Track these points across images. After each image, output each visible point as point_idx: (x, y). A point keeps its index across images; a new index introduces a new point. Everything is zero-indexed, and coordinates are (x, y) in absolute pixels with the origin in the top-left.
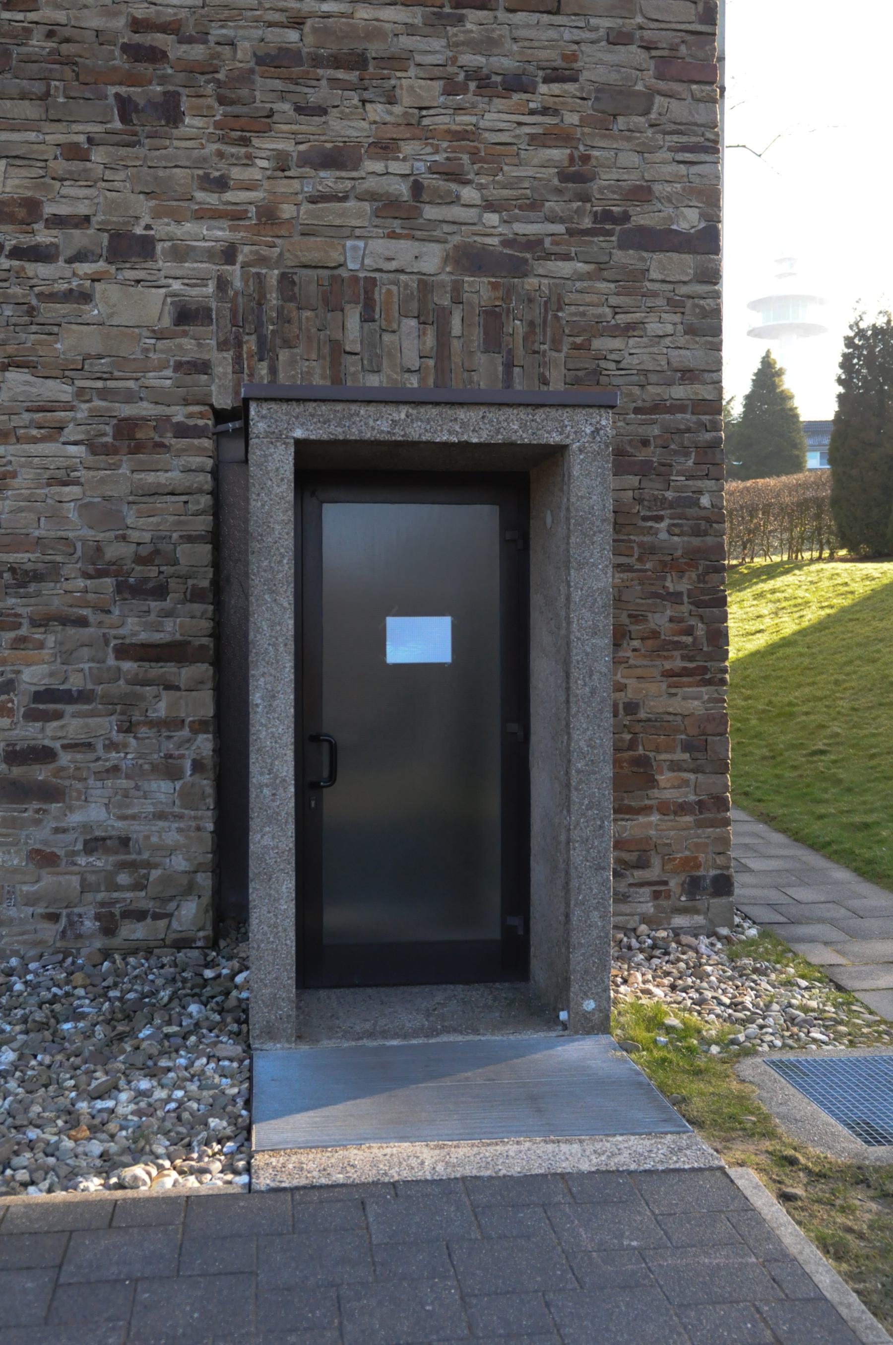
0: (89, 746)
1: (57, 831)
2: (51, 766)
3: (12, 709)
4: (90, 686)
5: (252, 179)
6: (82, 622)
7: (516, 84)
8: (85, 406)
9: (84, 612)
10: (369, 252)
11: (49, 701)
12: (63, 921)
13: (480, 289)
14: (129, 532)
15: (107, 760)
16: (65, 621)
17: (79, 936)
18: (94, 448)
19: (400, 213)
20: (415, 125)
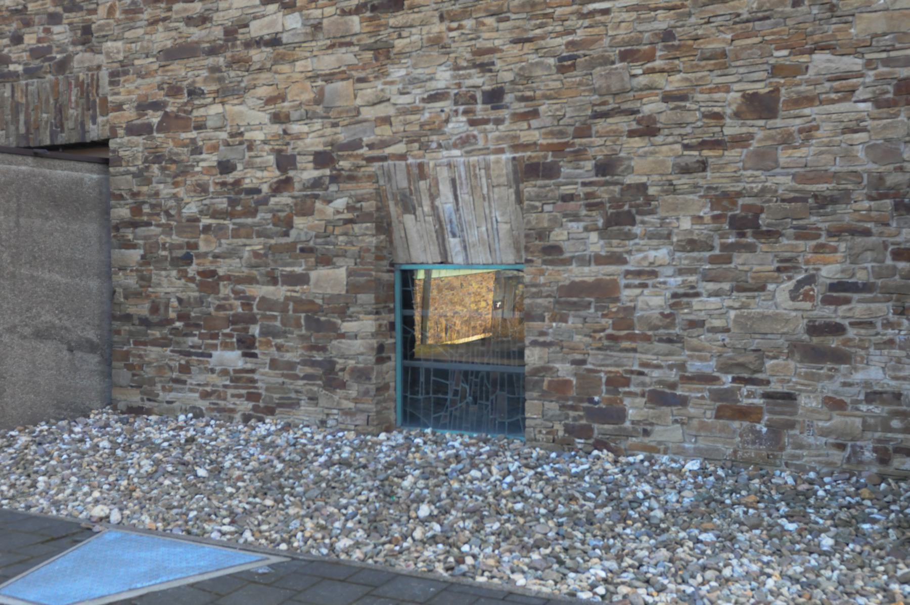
0: (871, 324)
1: (845, 384)
2: (841, 338)
3: (813, 296)
4: (872, 280)
6: (867, 233)
8: (871, 73)
9: (869, 225)
11: (840, 290)
12: (849, 450)
14: (905, 164)
15: (885, 335)
16: (854, 232)
17: (861, 463)
18: (878, 103)
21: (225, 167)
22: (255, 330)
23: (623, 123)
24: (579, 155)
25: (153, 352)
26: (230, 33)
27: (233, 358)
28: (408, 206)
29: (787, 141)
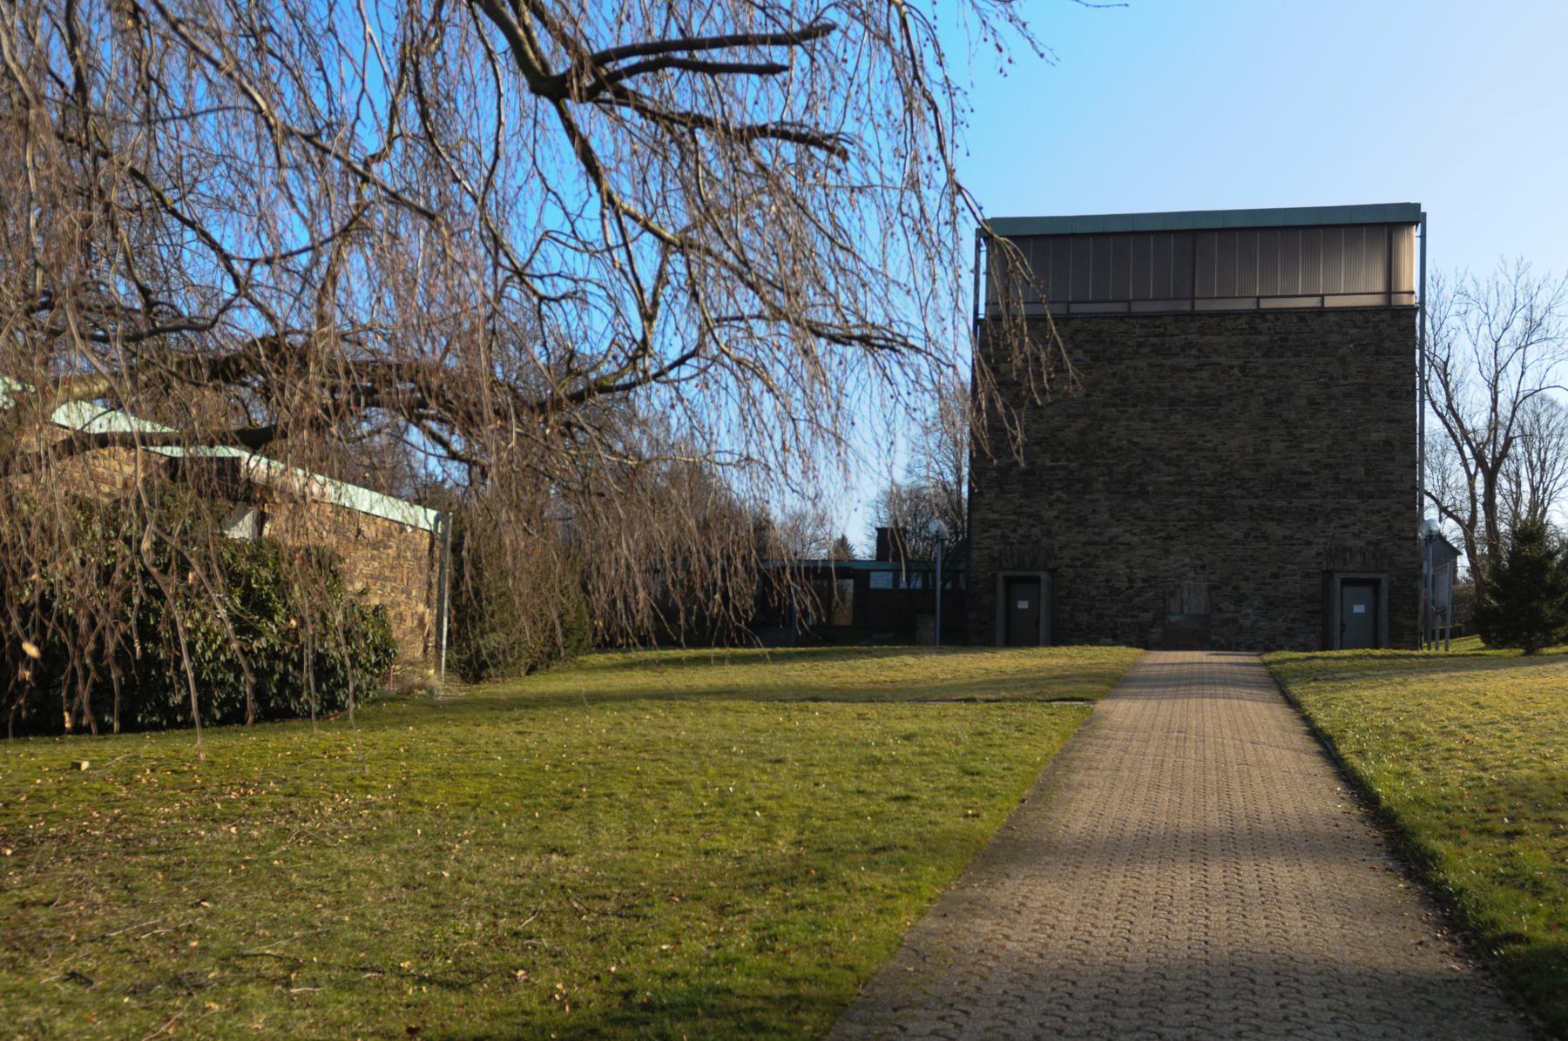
7: (1379, 512)
10: (1351, 542)
11: (1294, 620)
13: (1371, 548)
19: (1356, 535)
21: (1108, 581)
26: (1111, 539)
28: (1172, 595)
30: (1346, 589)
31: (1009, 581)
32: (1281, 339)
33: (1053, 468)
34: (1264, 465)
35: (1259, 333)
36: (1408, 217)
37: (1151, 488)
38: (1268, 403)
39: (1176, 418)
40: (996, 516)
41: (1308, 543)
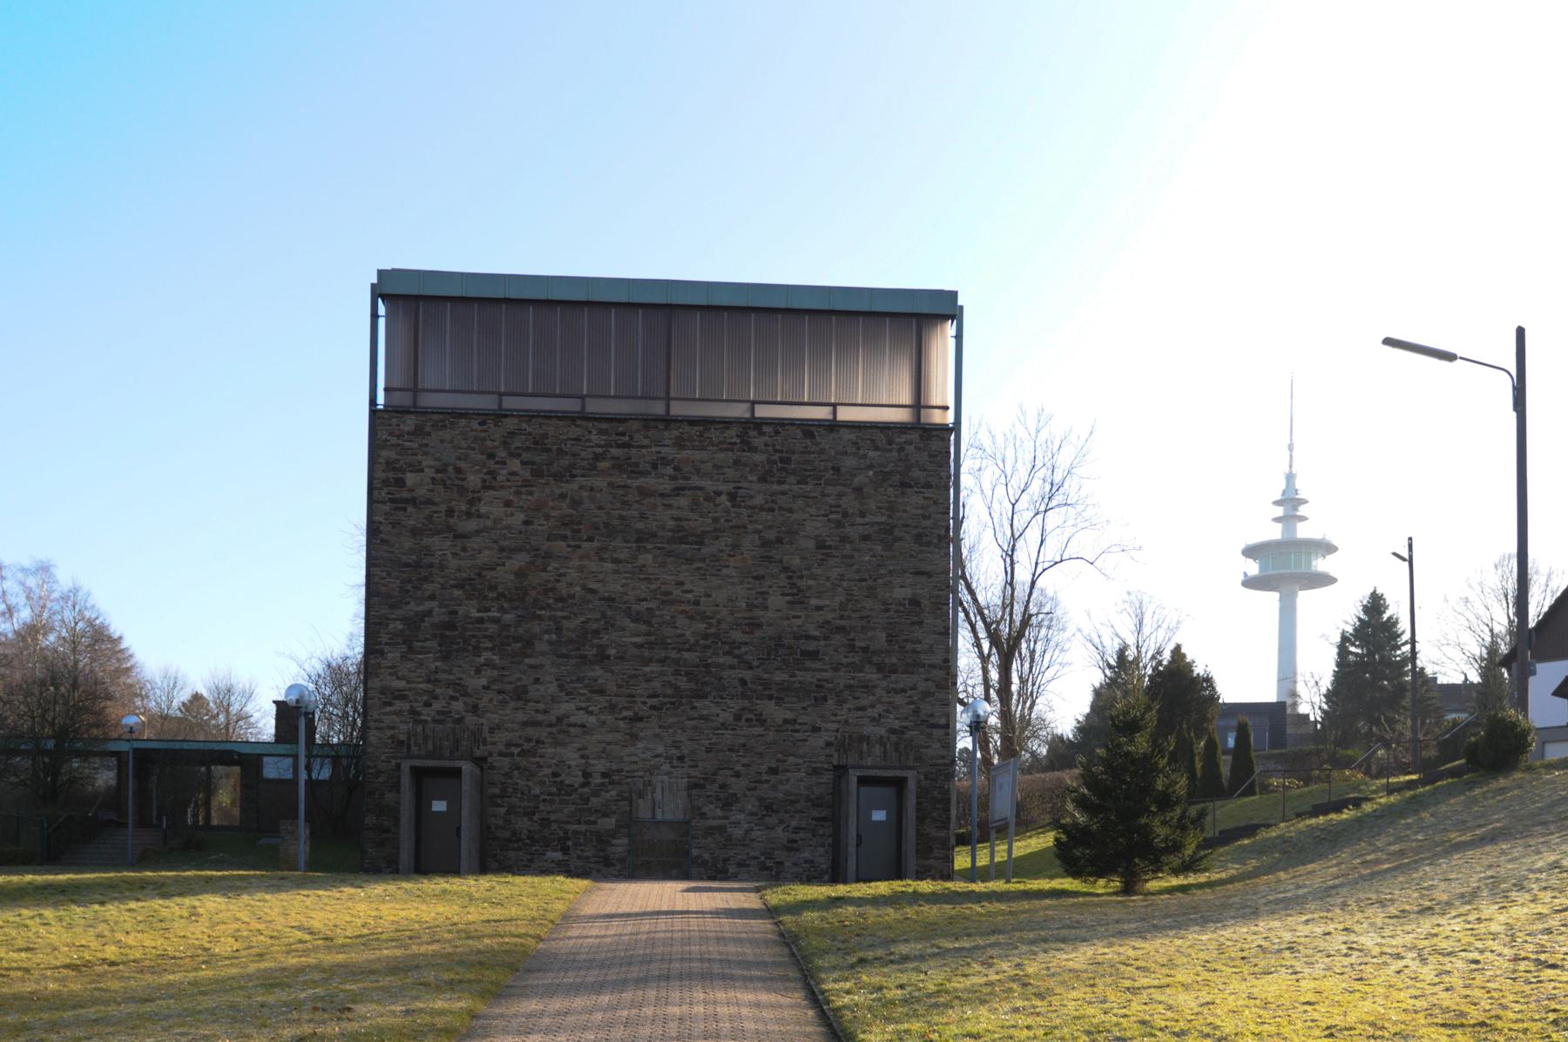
5: (843, 714)
7: (903, 691)
10: (869, 730)
11: (797, 830)
13: (894, 738)
19: (876, 721)
20: (879, 701)
21: (555, 775)
22: (570, 843)
23: (729, 772)
24: (713, 782)
25: (511, 854)
26: (560, 720)
27: (558, 855)
28: (641, 796)
29: (781, 782)
30: (862, 789)
31: (419, 774)
32: (782, 460)
33: (480, 621)
34: (759, 625)
35: (755, 450)
36: (939, 309)
37: (612, 652)
38: (765, 544)
39: (647, 559)
40: (403, 684)
41: (816, 729)
